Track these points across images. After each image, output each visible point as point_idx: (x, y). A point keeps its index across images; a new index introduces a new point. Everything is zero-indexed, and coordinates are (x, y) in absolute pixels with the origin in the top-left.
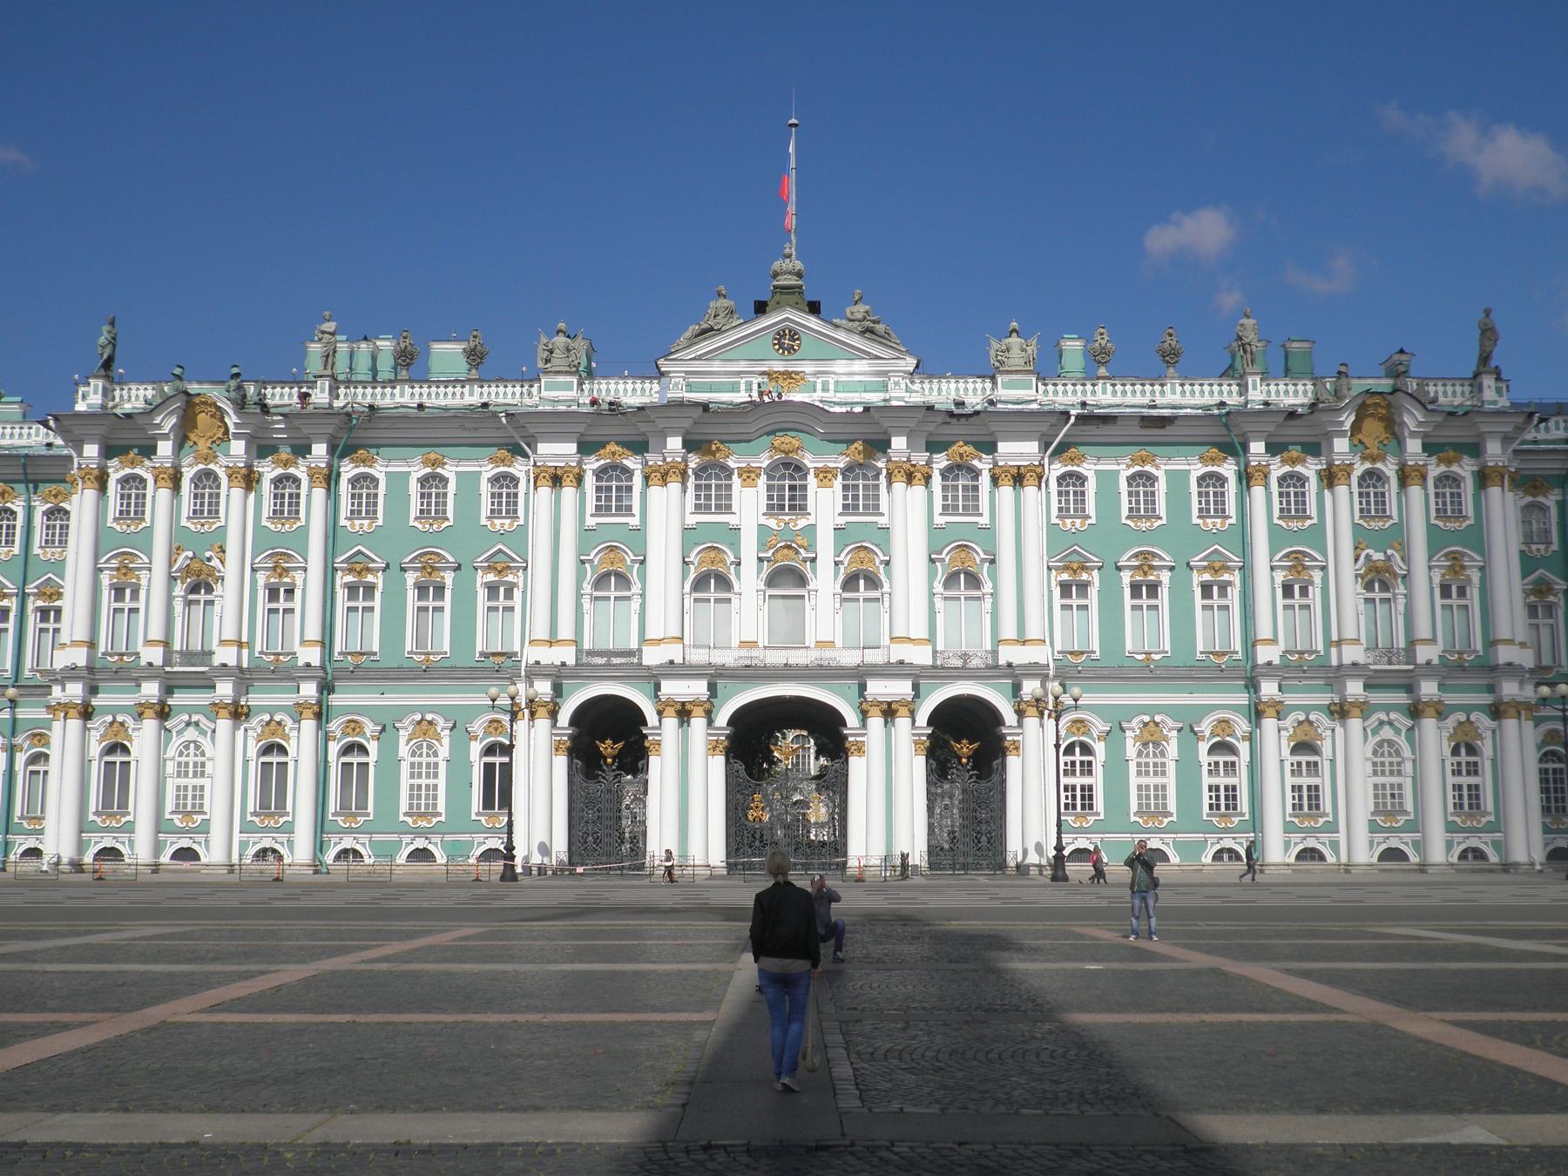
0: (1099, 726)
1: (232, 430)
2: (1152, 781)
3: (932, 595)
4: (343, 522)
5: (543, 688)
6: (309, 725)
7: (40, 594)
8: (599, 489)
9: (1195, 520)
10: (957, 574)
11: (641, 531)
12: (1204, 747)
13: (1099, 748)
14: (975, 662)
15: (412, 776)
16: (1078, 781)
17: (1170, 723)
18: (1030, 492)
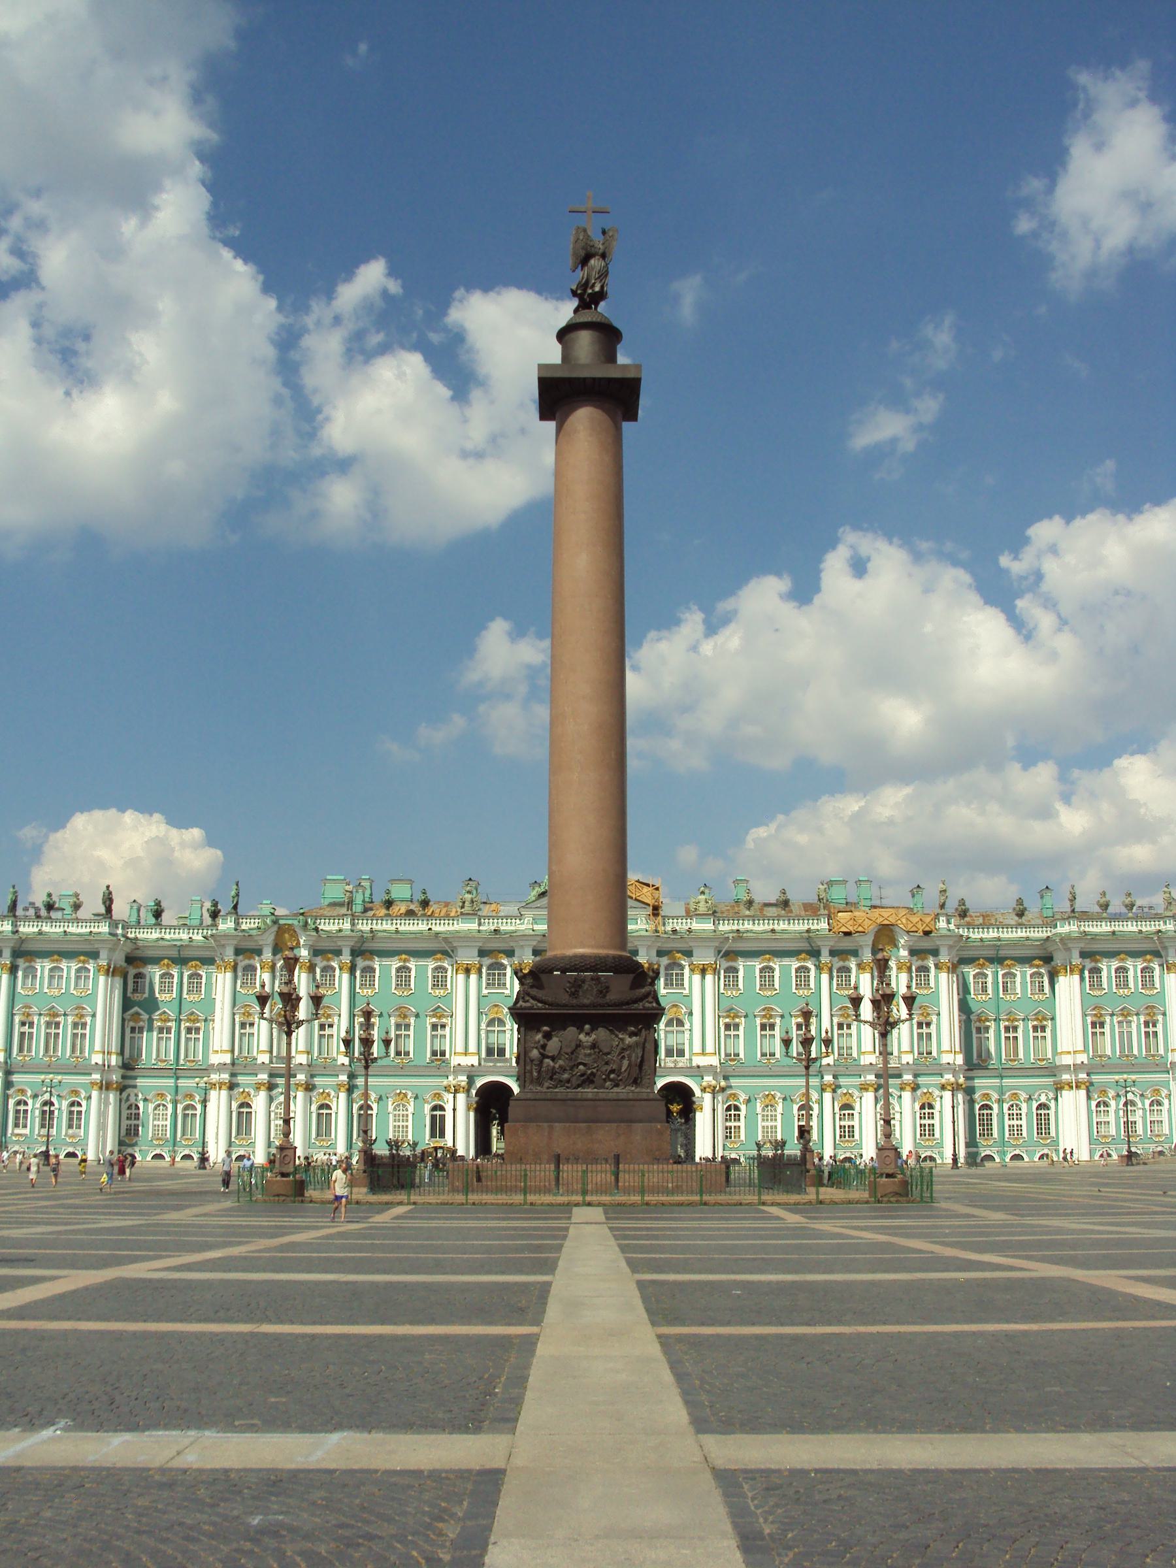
0: (743, 1097)
2: (769, 1124)
4: (358, 990)
5: (463, 1079)
7: (189, 1020)
8: (488, 974)
12: (796, 1107)
13: (743, 1107)
14: (680, 1065)
16: (733, 1124)
17: (779, 1094)
18: (709, 978)
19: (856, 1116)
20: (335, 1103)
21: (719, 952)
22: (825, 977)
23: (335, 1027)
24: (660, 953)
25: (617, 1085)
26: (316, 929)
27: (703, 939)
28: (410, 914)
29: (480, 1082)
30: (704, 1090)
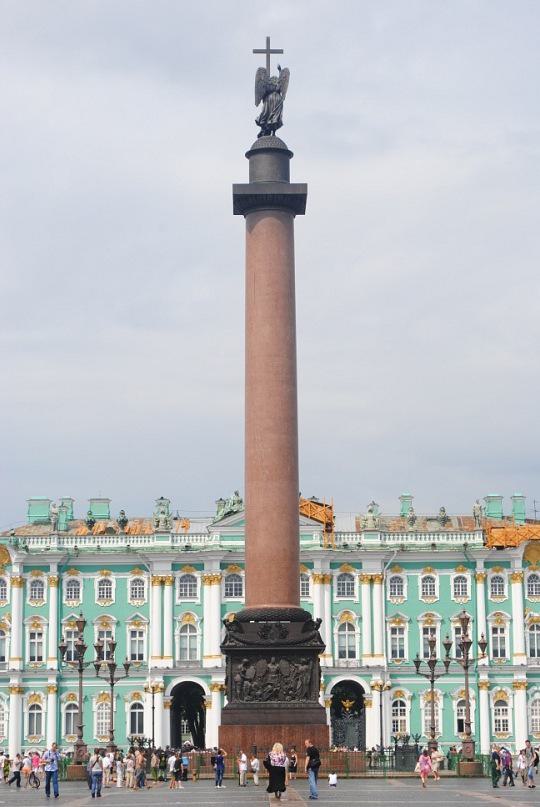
0: (408, 694)
1: (13, 560)
3: (333, 634)
4: (64, 602)
5: (159, 680)
6: (52, 697)
9: (453, 599)
10: (344, 624)
11: (201, 605)
12: (455, 703)
13: (408, 703)
15: (99, 718)
16: (399, 718)
17: (440, 692)
18: (377, 586)
19: (510, 711)
20: (44, 704)
21: (386, 564)
22: (480, 586)
23: (44, 636)
24: (333, 566)
25: (294, 698)
26: (26, 548)
27: (370, 552)
28: (109, 531)
29: (175, 682)
30: (372, 688)
